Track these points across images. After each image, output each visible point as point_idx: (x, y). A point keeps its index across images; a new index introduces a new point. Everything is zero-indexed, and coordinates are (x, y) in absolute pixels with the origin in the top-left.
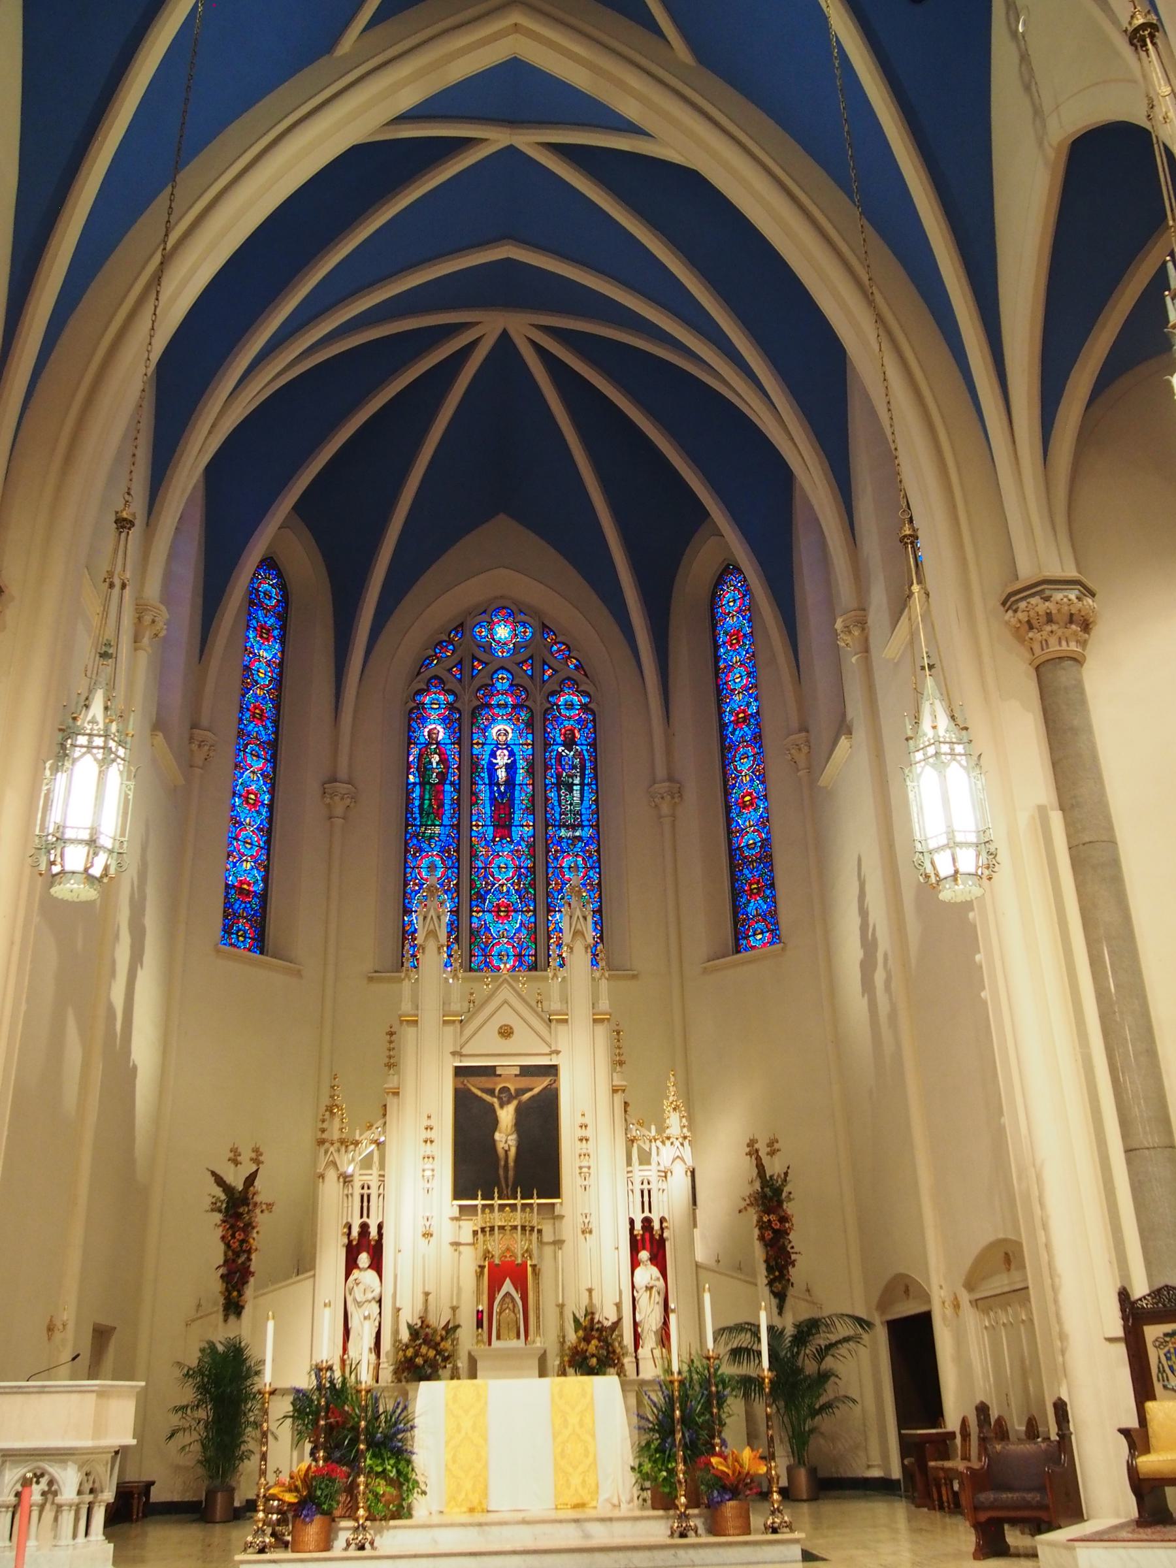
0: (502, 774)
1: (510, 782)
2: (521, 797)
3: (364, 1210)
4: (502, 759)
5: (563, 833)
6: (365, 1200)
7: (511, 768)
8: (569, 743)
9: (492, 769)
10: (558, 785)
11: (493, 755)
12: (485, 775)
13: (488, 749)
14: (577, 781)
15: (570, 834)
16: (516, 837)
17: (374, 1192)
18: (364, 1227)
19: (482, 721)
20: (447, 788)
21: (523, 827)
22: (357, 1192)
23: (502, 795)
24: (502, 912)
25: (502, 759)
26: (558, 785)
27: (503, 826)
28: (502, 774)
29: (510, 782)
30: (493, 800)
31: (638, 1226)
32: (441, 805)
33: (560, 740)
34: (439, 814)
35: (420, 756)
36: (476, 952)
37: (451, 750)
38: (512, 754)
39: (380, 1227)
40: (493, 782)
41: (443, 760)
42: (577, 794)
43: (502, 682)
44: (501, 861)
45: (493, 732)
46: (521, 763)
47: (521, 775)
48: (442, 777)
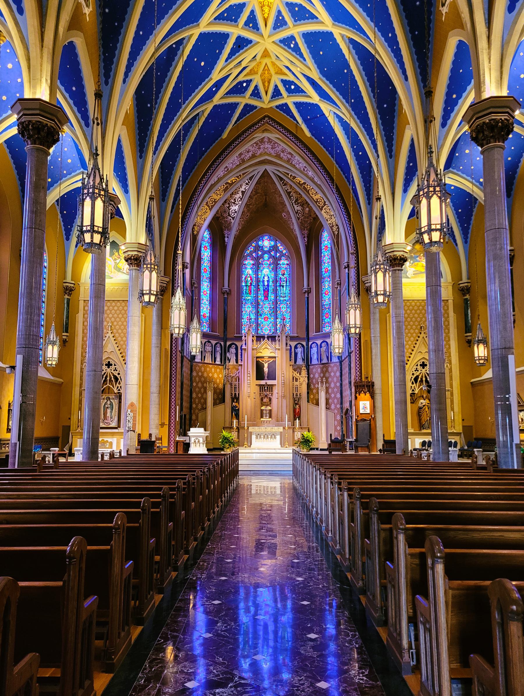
0: (266, 283)
1: (268, 285)
2: (271, 289)
3: (235, 391)
4: (266, 279)
5: (281, 299)
6: (235, 388)
7: (268, 281)
8: (283, 275)
9: (263, 281)
10: (280, 286)
11: (264, 278)
12: (262, 283)
13: (262, 276)
14: (285, 285)
15: (283, 299)
16: (269, 299)
17: (237, 386)
18: (235, 394)
19: (261, 269)
20: (252, 287)
21: (271, 297)
22: (233, 386)
23: (266, 289)
24: (266, 319)
25: (266, 279)
26: (280, 286)
27: (266, 298)
28: (266, 283)
29: (268, 285)
30: (264, 290)
31: (295, 395)
32: (251, 292)
33: (281, 273)
34: (250, 293)
35: (245, 278)
36: (259, 329)
37: (253, 276)
38: (268, 277)
39: (239, 394)
40: (264, 285)
41: (251, 279)
42: (285, 288)
43: (266, 256)
44: (266, 306)
45: (264, 272)
46: (271, 280)
47: (271, 283)
48: (251, 284)
